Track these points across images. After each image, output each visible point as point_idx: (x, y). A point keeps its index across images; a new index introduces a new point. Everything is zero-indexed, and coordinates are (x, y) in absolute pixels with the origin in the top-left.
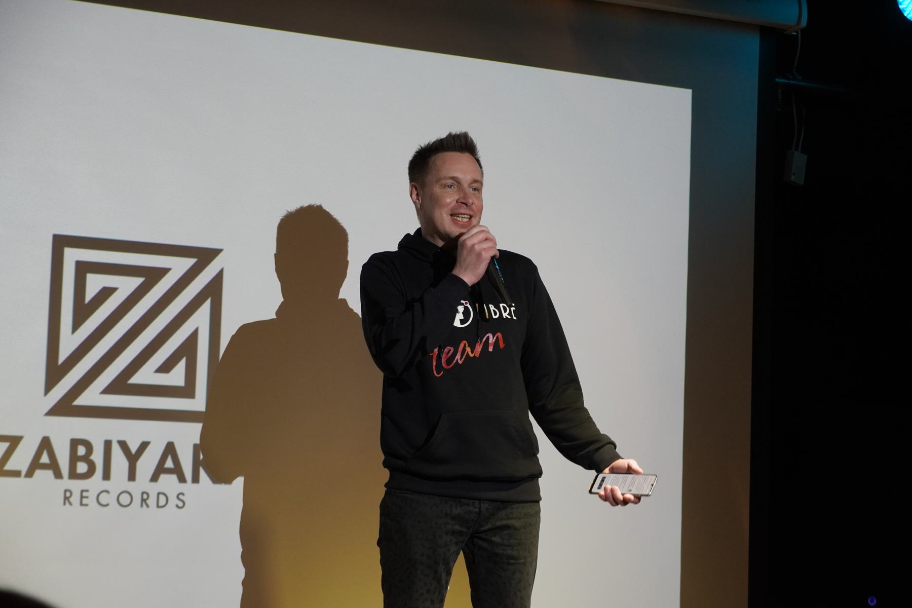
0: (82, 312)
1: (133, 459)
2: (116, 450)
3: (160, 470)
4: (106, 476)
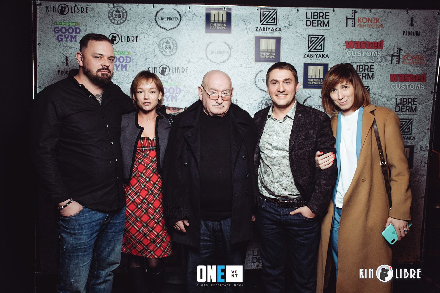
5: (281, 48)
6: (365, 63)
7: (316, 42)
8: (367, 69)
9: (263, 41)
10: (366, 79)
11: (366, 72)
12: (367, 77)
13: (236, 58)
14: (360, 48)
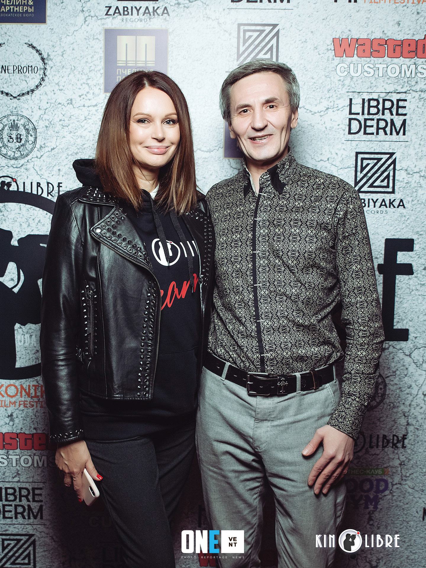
0: (363, 169)
1: (375, 203)
2: (371, 201)
3: (381, 205)
4: (369, 207)
5: (170, 58)
6: (383, 95)
7: (256, 43)
8: (390, 109)
9: (123, 41)
10: (386, 134)
11: (387, 116)
12: (388, 129)
13: (57, 84)
14: (371, 55)
